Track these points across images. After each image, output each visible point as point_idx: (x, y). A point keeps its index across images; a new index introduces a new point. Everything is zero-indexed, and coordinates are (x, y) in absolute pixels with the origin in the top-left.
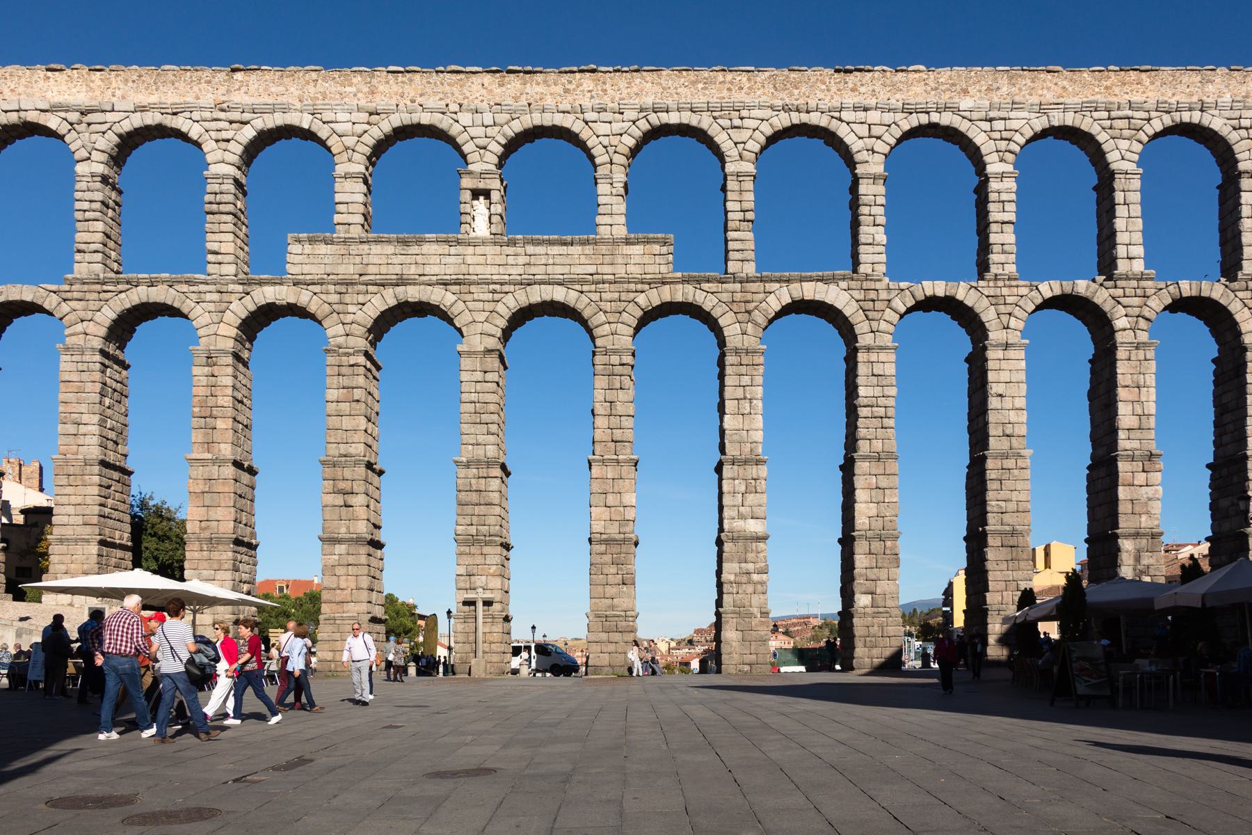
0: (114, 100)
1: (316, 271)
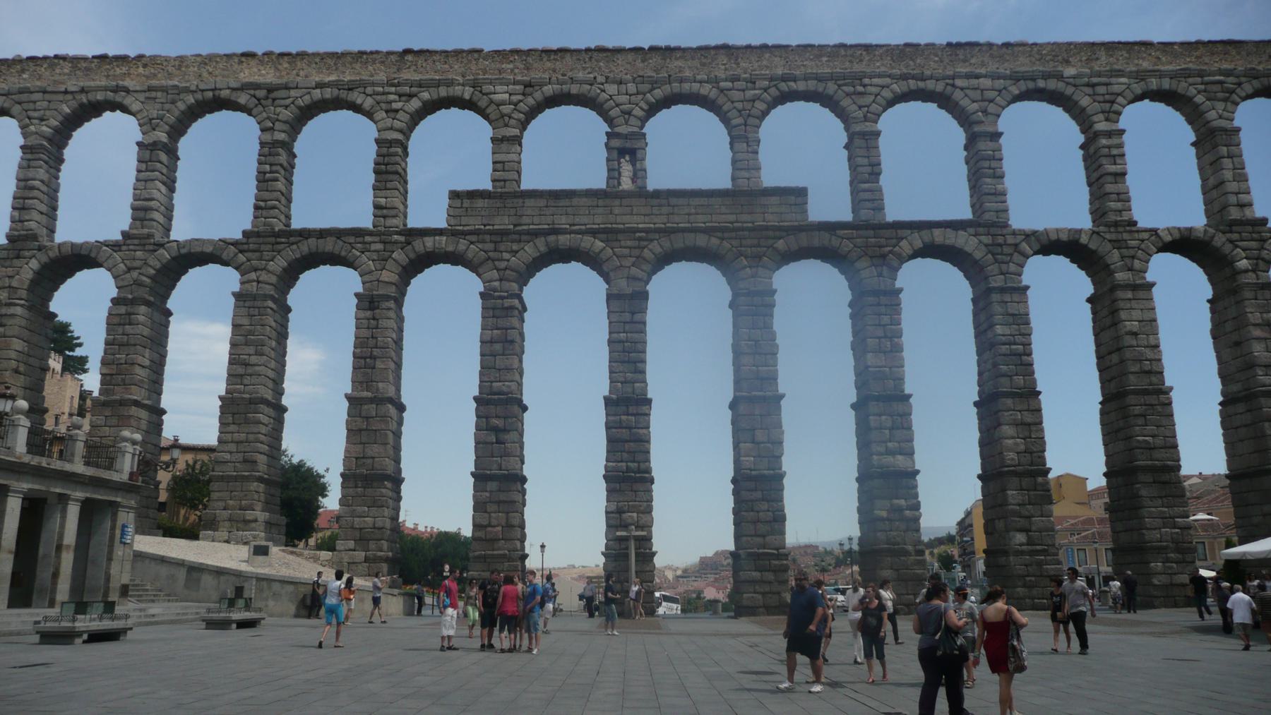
0: (299, 79)
1: (475, 223)
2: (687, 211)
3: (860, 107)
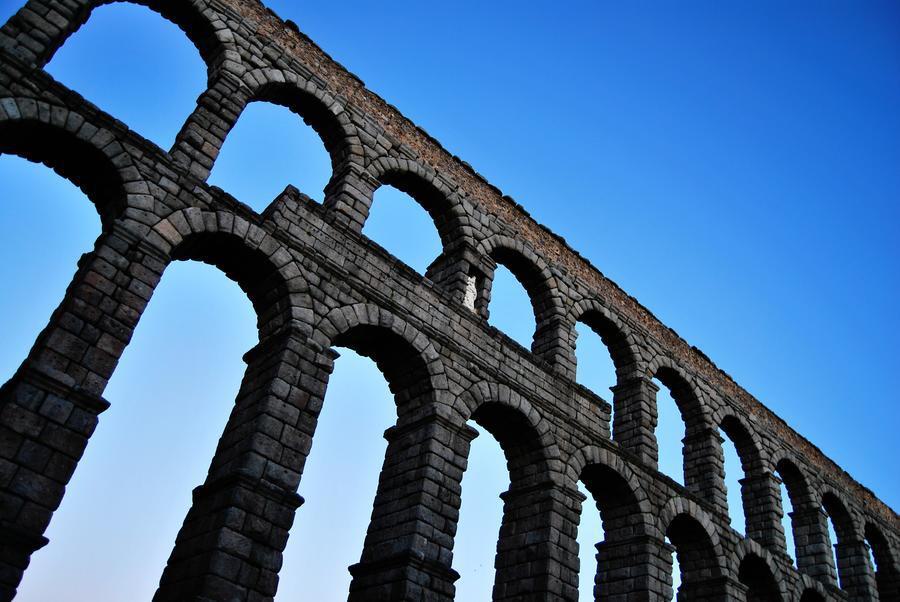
2: (516, 367)
3: (644, 360)
